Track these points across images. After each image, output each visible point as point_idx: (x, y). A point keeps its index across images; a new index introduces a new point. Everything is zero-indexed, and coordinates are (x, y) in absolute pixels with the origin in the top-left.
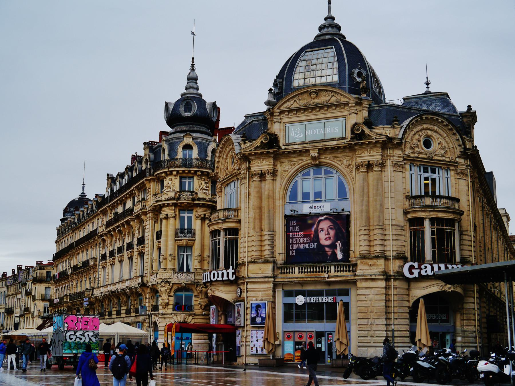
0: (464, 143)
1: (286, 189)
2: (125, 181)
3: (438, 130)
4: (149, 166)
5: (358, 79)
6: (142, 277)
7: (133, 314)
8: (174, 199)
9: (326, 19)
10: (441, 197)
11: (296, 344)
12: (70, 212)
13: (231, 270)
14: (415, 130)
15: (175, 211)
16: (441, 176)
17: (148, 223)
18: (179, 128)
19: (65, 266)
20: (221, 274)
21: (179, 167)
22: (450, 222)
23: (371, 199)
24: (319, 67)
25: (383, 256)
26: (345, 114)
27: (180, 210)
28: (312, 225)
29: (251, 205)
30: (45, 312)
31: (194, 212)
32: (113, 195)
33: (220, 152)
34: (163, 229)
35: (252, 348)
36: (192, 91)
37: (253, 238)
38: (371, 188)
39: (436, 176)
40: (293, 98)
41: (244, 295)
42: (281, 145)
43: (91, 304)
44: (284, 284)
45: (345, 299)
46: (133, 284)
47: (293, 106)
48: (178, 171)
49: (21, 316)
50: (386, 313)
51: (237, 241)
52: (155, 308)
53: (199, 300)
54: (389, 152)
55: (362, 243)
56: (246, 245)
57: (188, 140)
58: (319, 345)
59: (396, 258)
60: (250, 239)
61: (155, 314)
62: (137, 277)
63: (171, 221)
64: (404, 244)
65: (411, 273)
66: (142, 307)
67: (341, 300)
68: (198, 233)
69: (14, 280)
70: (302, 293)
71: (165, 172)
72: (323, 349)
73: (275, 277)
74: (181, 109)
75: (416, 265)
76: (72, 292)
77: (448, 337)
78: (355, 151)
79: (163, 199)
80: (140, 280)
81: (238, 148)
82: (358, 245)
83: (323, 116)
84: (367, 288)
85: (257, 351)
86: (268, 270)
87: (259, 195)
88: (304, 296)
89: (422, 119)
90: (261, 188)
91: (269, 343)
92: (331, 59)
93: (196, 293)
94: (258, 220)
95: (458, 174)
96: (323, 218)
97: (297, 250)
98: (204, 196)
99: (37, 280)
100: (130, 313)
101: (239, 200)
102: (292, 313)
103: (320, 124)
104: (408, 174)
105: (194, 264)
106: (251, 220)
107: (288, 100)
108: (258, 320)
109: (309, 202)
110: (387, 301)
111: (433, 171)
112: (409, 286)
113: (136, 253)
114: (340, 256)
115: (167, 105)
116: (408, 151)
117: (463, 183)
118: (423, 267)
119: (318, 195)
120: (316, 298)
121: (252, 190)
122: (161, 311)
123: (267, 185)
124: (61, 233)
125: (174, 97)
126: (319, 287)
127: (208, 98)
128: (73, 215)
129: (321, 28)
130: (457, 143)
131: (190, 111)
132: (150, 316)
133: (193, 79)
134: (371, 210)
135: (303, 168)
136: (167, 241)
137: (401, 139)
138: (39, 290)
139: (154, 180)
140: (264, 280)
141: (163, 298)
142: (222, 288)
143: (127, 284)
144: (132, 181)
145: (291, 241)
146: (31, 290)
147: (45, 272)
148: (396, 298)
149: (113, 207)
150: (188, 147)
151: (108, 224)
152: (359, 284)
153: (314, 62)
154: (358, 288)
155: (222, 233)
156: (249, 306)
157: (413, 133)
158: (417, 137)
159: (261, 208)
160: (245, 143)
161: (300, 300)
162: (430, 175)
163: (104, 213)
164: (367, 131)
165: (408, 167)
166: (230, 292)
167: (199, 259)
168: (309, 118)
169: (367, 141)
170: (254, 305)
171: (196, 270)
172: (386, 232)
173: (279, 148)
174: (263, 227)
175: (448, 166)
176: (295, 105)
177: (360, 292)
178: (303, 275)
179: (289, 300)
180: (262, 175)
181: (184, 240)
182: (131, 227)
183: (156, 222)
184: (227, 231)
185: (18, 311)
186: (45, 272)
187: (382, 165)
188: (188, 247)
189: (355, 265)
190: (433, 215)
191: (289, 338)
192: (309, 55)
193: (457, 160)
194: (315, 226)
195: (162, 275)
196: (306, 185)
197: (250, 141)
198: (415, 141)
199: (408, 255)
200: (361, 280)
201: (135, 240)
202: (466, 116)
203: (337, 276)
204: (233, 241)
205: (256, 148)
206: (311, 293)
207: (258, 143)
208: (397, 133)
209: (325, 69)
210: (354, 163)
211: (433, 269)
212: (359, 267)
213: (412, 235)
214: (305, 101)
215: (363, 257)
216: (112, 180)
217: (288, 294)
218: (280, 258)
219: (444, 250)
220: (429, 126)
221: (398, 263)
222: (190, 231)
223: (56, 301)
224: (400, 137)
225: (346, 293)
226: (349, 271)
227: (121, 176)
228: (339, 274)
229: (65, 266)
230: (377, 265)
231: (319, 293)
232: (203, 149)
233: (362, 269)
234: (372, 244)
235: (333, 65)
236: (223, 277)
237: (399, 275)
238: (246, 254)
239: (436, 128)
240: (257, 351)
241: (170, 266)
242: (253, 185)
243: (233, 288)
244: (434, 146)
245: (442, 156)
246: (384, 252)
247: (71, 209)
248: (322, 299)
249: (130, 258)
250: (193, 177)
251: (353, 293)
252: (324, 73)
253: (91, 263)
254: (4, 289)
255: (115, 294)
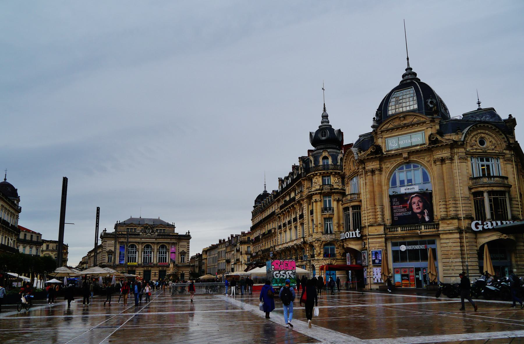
0: (508, 140)
1: (389, 179)
2: (289, 181)
3: (489, 133)
4: (303, 171)
5: (431, 106)
6: (303, 238)
7: (299, 261)
8: (319, 190)
9: (406, 70)
10: (494, 177)
11: (402, 276)
12: (258, 202)
13: (357, 231)
14: (472, 135)
15: (320, 197)
16: (493, 163)
17: (305, 206)
18: (319, 147)
19: (258, 233)
20: (351, 234)
21: (321, 170)
22: (502, 193)
23: (445, 181)
24: (404, 101)
25: (456, 217)
26: (423, 128)
27: (323, 196)
28: (407, 200)
29: (367, 190)
30: (248, 261)
31: (332, 197)
32: (283, 190)
33: (346, 159)
34: (314, 208)
35: (374, 279)
36: (325, 124)
37: (370, 211)
38: (445, 174)
39: (490, 163)
40: (389, 122)
41: (367, 246)
42: (383, 152)
43: (275, 255)
44: (392, 238)
45: (433, 246)
46: (298, 242)
47: (390, 127)
48: (320, 173)
49: (235, 264)
50: (462, 254)
51: (360, 213)
52: (313, 256)
53: (339, 250)
54: (456, 150)
55: (441, 210)
56: (366, 215)
57: (325, 154)
58: (417, 276)
59: (465, 218)
60: (368, 211)
61: (313, 260)
62: (300, 238)
63: (319, 203)
64: (470, 209)
65: (477, 228)
66: (305, 256)
67: (430, 247)
68: (335, 209)
69: (230, 243)
70: (404, 244)
71: (313, 174)
72: (420, 279)
73: (385, 234)
74: (320, 135)
75: (480, 222)
76: (263, 248)
77: (507, 269)
78: (432, 151)
79: (313, 190)
80: (302, 240)
81: (357, 156)
82: (439, 211)
83: (409, 131)
84: (447, 239)
85: (378, 281)
86: (381, 230)
87: (372, 184)
88: (405, 245)
89: (477, 127)
90: (373, 179)
91: (385, 275)
92: (412, 95)
93: (337, 246)
94: (372, 199)
95: (505, 161)
96: (414, 196)
97: (399, 217)
98: (337, 187)
99: (242, 243)
100: (298, 260)
101: (359, 188)
102: (398, 256)
103: (408, 136)
104: (469, 163)
105: (335, 229)
106: (368, 200)
107: (386, 124)
108: (377, 261)
109: (404, 186)
110: (462, 246)
111: (488, 160)
112: (476, 236)
113: (299, 224)
114: (427, 219)
115: (311, 133)
116: (469, 149)
117: (509, 167)
118: (485, 223)
119: (410, 181)
120: (413, 247)
121: (367, 181)
122: (316, 258)
123: (376, 178)
124: (255, 214)
125: (315, 129)
126: (415, 239)
127: (335, 127)
128: (261, 203)
129: (403, 76)
130: (503, 140)
131: (325, 136)
132: (310, 261)
133: (325, 117)
134: (446, 188)
135: (399, 165)
136: (317, 215)
137: (463, 141)
138: (244, 248)
139: (306, 179)
140: (379, 236)
141: (317, 250)
142: (353, 242)
143: (295, 242)
144: (293, 181)
145: (395, 211)
146: (239, 248)
147: (246, 237)
148: (468, 244)
149: (284, 197)
150: (325, 158)
151: (281, 207)
152: (441, 236)
153: (401, 98)
154: (441, 239)
155: (351, 209)
156: (370, 252)
157: (471, 136)
158: (474, 139)
159: (374, 192)
160: (360, 153)
161: (403, 248)
162: (485, 163)
163: (278, 201)
164: (439, 138)
165: (469, 159)
166: (358, 244)
167: (337, 225)
168: (400, 133)
169: (440, 145)
170: (373, 252)
171: (336, 232)
172: (458, 202)
173: (383, 154)
174: (376, 204)
175: (497, 156)
176: (391, 126)
177: (442, 241)
178: (404, 232)
179: (396, 248)
180: (373, 172)
181: (327, 214)
182: (295, 208)
183: (310, 204)
184: (354, 207)
185: (233, 261)
186: (246, 237)
187: (451, 159)
188: (330, 219)
189: (438, 224)
190: (490, 189)
191: (397, 272)
192: (398, 94)
193: (504, 151)
194: (409, 201)
195: (315, 236)
196: (401, 176)
197: (364, 151)
198: (473, 142)
199: (474, 216)
200: (442, 233)
201: (298, 216)
202: (508, 122)
203: (426, 232)
204: (357, 213)
205: (368, 155)
206: (409, 244)
207: (369, 152)
208: (460, 137)
209: (409, 103)
210: (432, 159)
211: (492, 224)
212: (441, 226)
213: (476, 203)
214: (396, 123)
215: (443, 219)
216: (281, 181)
217: (394, 244)
218: (388, 222)
219: (499, 212)
220: (482, 131)
221: (467, 221)
222: (330, 209)
223: (254, 254)
224: (462, 140)
225: (433, 242)
226: (434, 228)
227: (287, 178)
228: (428, 230)
229: (258, 233)
230: (453, 224)
231: (415, 243)
232: (335, 159)
233: (443, 227)
234: (448, 210)
235: (413, 98)
236: (353, 235)
237: (469, 229)
238: (366, 221)
239: (487, 132)
240: (378, 281)
241: (319, 230)
242: (368, 178)
243: (360, 242)
244: (487, 144)
245: (493, 150)
246: (457, 215)
247: (259, 200)
248: (417, 247)
249: (296, 227)
250: (330, 176)
251: (438, 242)
252: (408, 104)
253: (273, 231)
254: (224, 249)
255: (288, 249)
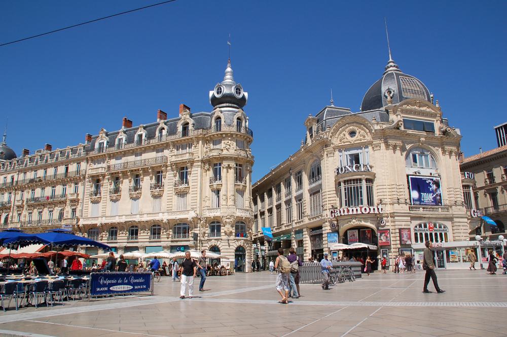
65: (474, 215)
155: (364, 182)
183: (209, 170)
184: (368, 180)
